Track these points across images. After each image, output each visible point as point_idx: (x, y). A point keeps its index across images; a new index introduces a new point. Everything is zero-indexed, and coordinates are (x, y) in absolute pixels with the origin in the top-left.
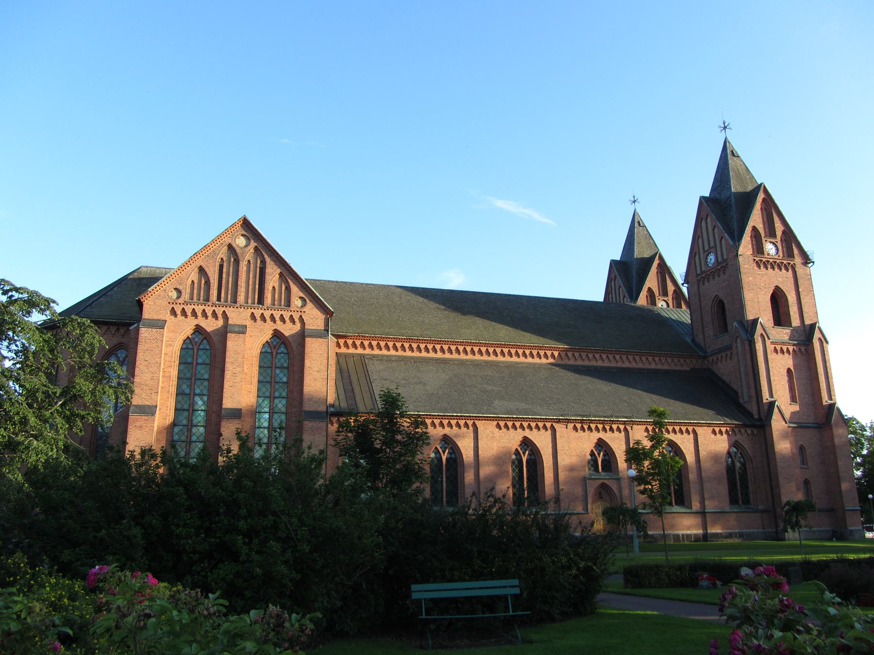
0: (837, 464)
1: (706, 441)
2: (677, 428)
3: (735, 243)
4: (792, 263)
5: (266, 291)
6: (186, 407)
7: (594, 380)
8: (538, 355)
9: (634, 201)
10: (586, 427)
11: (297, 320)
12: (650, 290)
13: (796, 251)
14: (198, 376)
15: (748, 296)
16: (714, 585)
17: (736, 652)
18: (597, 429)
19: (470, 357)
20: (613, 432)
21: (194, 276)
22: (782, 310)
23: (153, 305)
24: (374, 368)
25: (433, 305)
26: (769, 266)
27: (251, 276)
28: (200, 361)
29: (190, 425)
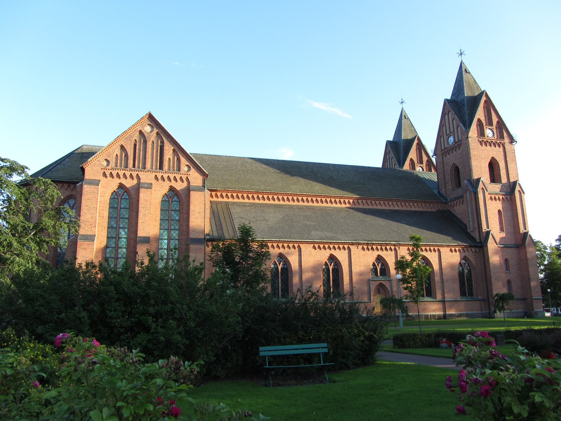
0: (528, 270)
1: (446, 256)
2: (428, 248)
4: (503, 142)
5: (164, 161)
6: (114, 236)
7: (375, 218)
8: (340, 202)
9: (402, 102)
10: (370, 247)
11: (184, 180)
12: (411, 160)
13: (505, 134)
14: (122, 216)
15: (474, 163)
16: (450, 346)
17: (462, 383)
18: (377, 249)
19: (296, 203)
20: (387, 251)
21: (118, 151)
22: (495, 172)
23: (92, 170)
24: (235, 211)
25: (272, 170)
26: (488, 144)
27: (155, 151)
28: (122, 206)
29: (117, 248)
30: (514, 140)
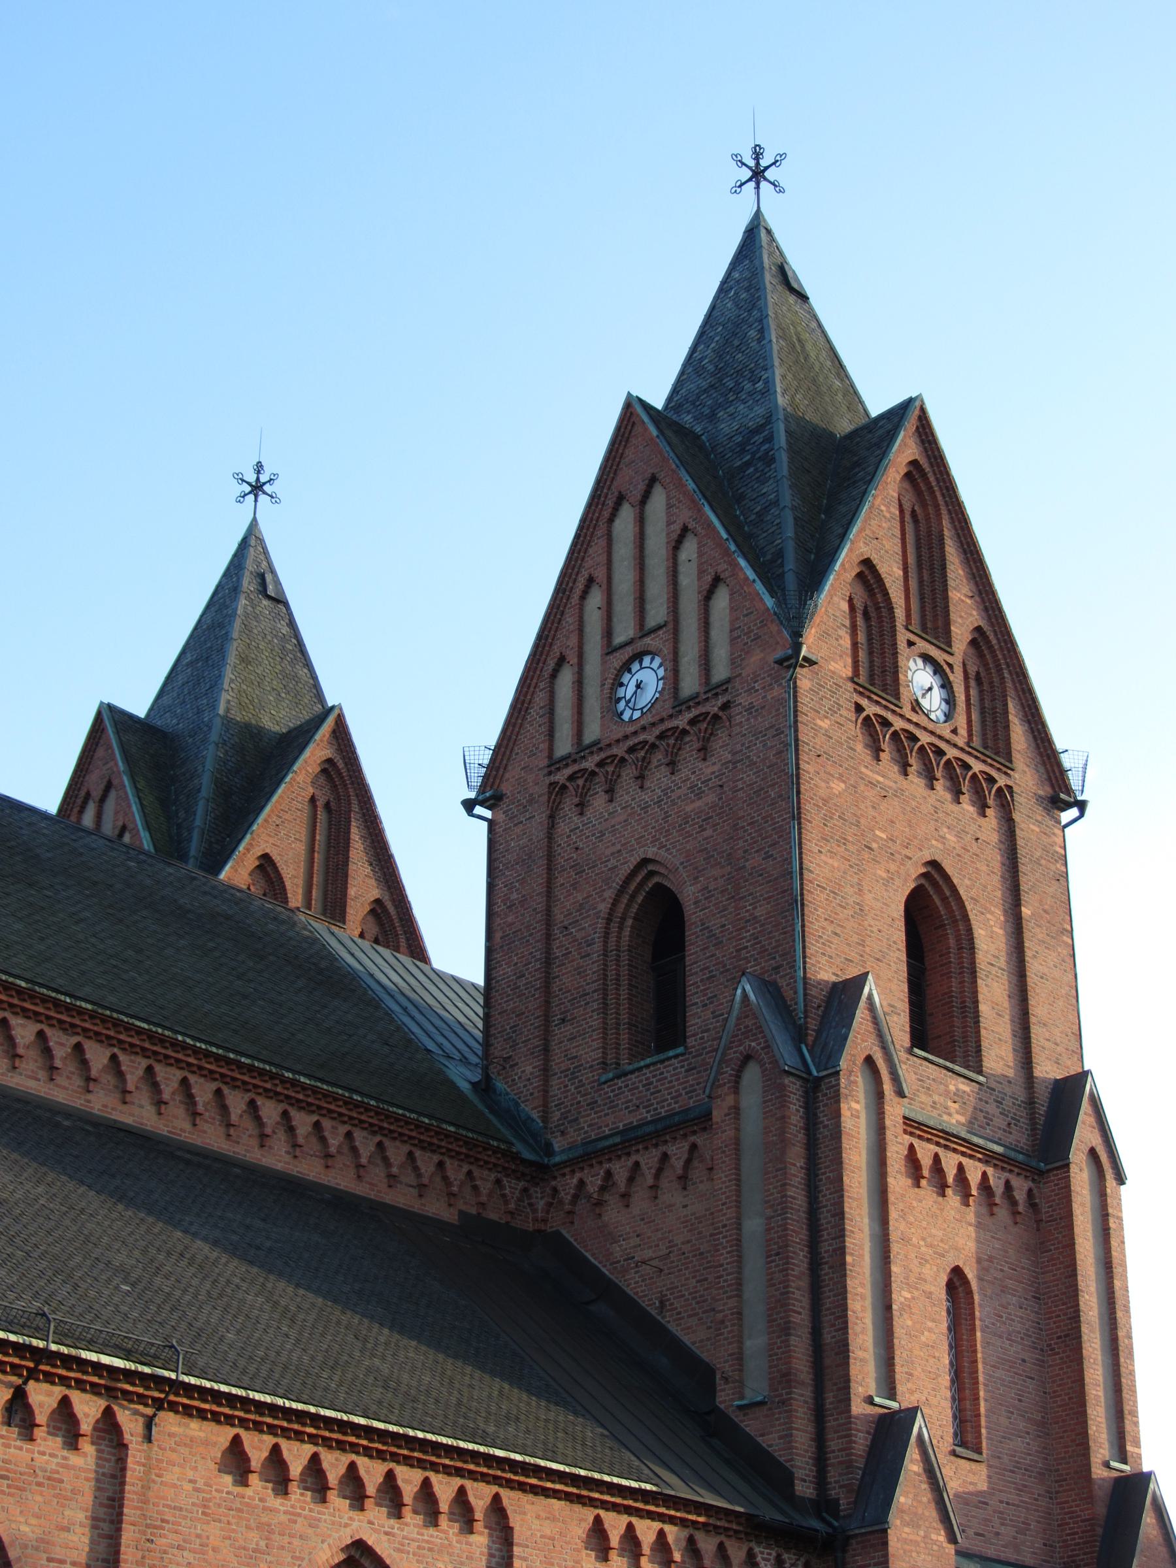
2: (409, 1479)
3: (781, 601)
4: (1002, 781)
9: (257, 488)
15: (822, 863)
30: (1068, 790)
